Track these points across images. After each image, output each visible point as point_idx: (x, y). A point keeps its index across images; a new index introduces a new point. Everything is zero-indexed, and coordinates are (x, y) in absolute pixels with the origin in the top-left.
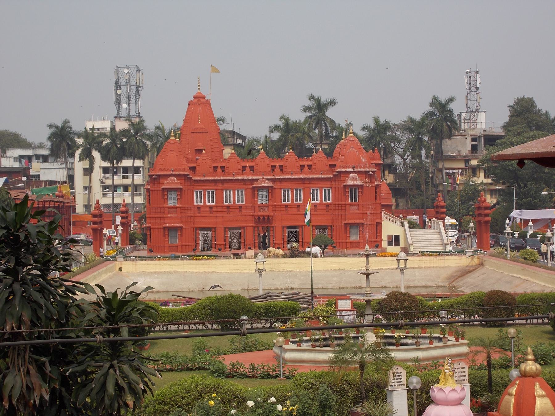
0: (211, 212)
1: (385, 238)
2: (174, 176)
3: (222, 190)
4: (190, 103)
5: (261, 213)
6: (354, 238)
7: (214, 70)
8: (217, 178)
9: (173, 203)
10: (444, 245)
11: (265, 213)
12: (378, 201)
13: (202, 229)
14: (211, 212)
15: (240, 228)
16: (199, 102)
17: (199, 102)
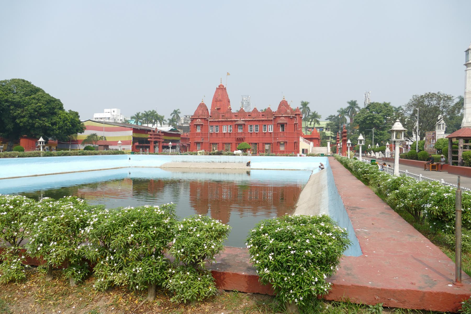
0: (217, 136)
1: (301, 150)
2: (199, 118)
3: (222, 126)
4: (217, 89)
5: (239, 137)
6: (282, 148)
7: (228, 74)
8: (220, 120)
9: (199, 131)
10: (328, 153)
11: (241, 136)
12: (296, 131)
13: (212, 144)
14: (217, 136)
15: (229, 144)
16: (221, 89)
17: (221, 89)
